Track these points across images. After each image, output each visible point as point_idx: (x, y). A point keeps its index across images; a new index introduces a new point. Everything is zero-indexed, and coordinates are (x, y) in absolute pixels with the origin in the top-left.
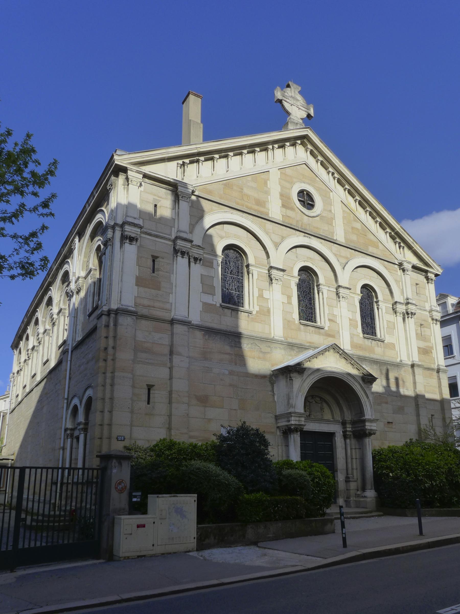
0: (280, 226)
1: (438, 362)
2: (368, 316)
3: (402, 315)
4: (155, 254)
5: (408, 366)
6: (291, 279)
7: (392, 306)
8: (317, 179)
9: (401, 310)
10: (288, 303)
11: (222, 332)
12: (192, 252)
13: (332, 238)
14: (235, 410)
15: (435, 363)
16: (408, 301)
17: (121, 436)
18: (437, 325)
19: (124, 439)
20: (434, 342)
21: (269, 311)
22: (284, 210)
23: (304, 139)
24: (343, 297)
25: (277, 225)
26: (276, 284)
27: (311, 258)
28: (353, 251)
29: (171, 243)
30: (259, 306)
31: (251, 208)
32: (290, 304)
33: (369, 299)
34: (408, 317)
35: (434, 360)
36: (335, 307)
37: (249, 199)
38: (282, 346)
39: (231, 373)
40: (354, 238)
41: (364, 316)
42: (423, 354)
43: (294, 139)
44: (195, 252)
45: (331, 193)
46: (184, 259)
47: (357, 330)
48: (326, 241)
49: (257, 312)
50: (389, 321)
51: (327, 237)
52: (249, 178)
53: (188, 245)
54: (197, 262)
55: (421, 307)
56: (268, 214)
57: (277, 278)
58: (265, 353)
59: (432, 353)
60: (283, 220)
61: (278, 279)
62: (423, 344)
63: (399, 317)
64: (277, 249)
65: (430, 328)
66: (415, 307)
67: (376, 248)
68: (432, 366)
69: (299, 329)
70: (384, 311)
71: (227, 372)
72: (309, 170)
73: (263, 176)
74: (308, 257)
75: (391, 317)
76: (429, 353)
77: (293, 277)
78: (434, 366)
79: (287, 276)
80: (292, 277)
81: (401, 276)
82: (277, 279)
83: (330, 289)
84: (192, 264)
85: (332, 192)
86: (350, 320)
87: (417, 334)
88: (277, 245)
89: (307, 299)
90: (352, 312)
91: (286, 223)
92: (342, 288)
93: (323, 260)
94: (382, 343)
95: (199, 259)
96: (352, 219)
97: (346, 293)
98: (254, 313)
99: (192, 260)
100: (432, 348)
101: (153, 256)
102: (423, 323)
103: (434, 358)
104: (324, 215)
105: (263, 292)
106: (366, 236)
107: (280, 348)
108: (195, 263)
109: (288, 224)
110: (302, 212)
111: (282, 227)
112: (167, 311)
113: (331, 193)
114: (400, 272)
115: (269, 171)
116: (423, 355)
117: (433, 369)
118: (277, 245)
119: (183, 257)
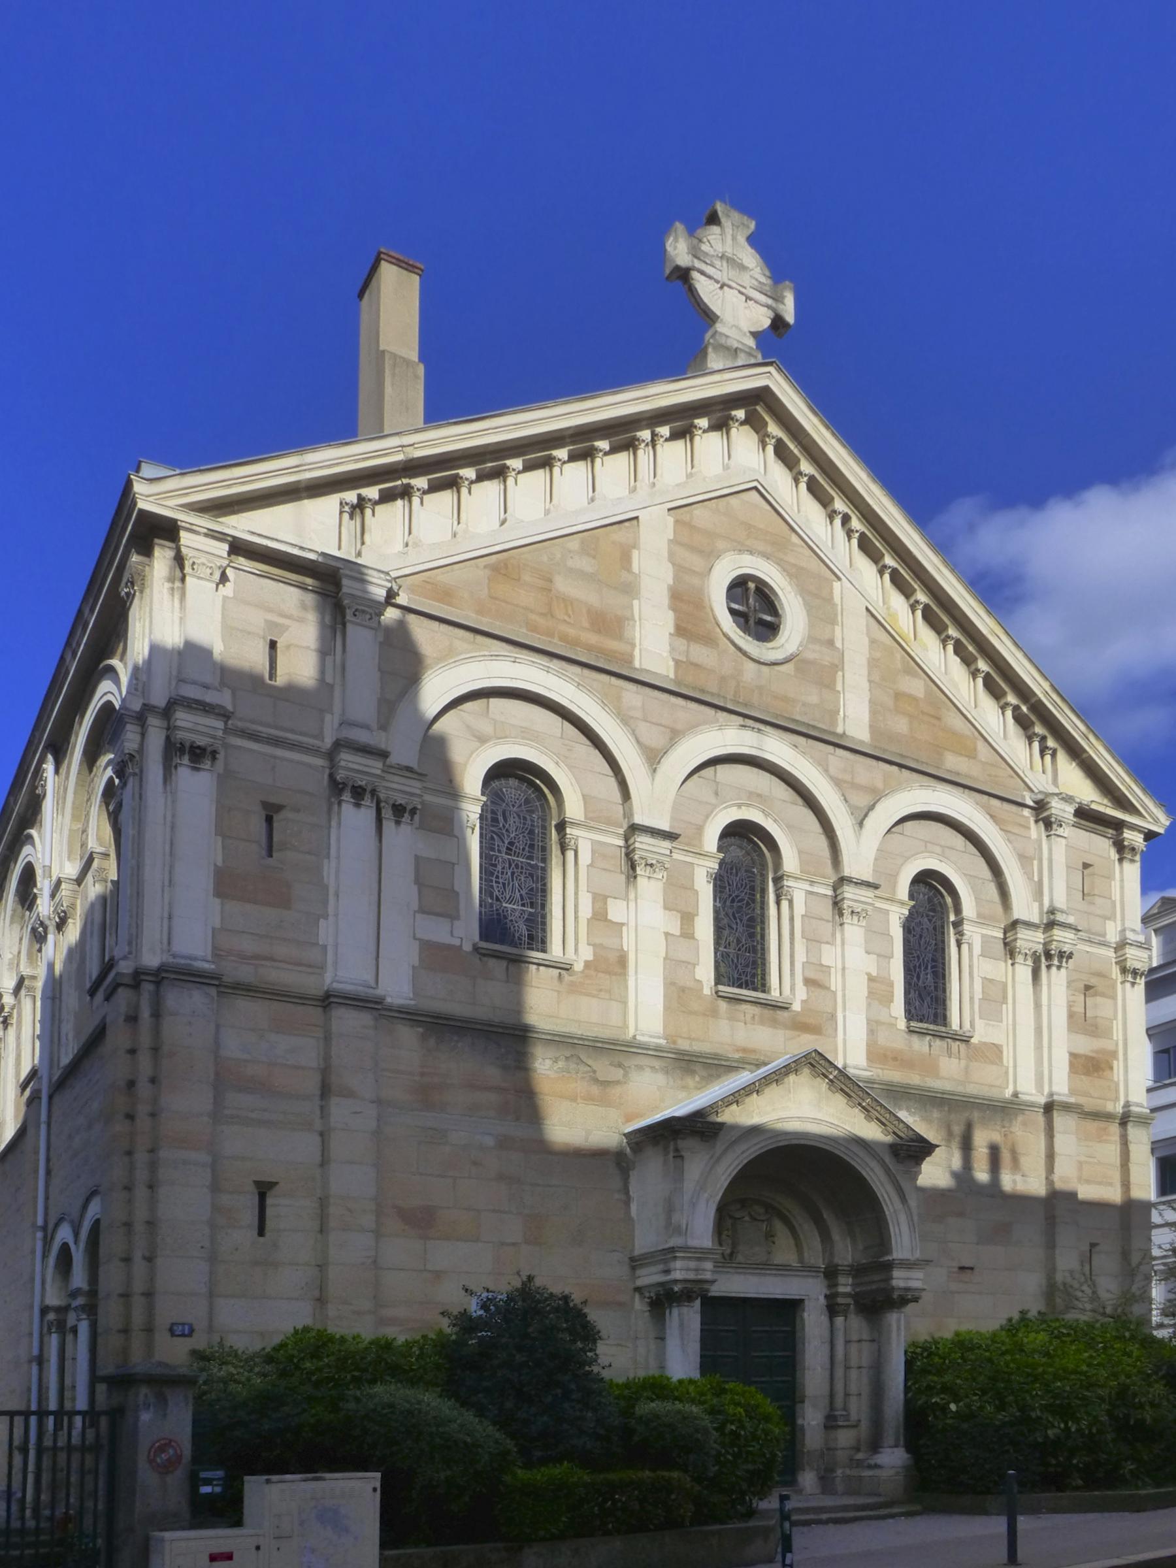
0: (665, 696)
1: (1127, 1095)
2: (926, 968)
3: (1030, 962)
4: (273, 799)
5: (1036, 1109)
6: (695, 861)
7: (1002, 936)
8: (795, 538)
11: (479, 1027)
12: (387, 788)
13: (832, 729)
14: (514, 1244)
15: (1117, 1099)
16: (1052, 917)
17: (183, 1324)
18: (1136, 986)
19: (192, 1331)
20: (1121, 1037)
21: (622, 961)
22: (681, 643)
23: (757, 404)
24: (853, 912)
25: (656, 693)
27: (759, 796)
28: (895, 769)
29: (319, 762)
30: (594, 945)
31: (574, 643)
32: (689, 938)
33: (933, 917)
34: (1049, 967)
35: (1117, 1091)
36: (828, 943)
37: (570, 612)
38: (657, 1064)
39: (504, 1143)
40: (901, 725)
41: (915, 967)
42: (1084, 1074)
43: (722, 407)
44: (397, 788)
45: (837, 585)
46: (363, 809)
47: (889, 1008)
48: (810, 741)
49: (587, 964)
50: (991, 981)
51: (814, 727)
52: (574, 544)
53: (375, 766)
54: (403, 820)
55: (1093, 934)
56: (629, 660)
57: (653, 859)
58: (606, 1084)
59: (1111, 1068)
60: (676, 676)
61: (654, 862)
62: (1086, 1045)
63: (1022, 966)
64: (655, 770)
65: (1114, 997)
66: (1072, 936)
67: (967, 756)
68: (1110, 1107)
69: (714, 1013)
70: (977, 949)
71: (490, 1141)
72: (768, 507)
73: (619, 535)
75: (998, 969)
76: (1103, 1071)
77: (702, 857)
78: (1115, 1107)
79: (685, 853)
80: (698, 856)
81: (1039, 841)
82: (650, 862)
83: (815, 889)
84: (389, 826)
85: (839, 579)
86: (871, 979)
87: (1071, 1015)
88: (654, 758)
89: (741, 920)
90: (879, 955)
91: (687, 686)
92: (852, 885)
93: (799, 801)
94: (963, 1046)
95: (409, 807)
96: (899, 666)
97: (863, 899)
98: (578, 967)
99: (387, 813)
100: (1114, 1054)
101: (266, 805)
103: (1117, 1084)
104: (809, 655)
105: (606, 904)
107: (652, 1068)
108: (398, 823)
109: (694, 688)
110: (739, 649)
111: (673, 699)
112: (309, 970)
113: (837, 585)
114: (1036, 831)
115: (637, 518)
117: (1108, 1117)
118: (654, 758)
119: (358, 805)
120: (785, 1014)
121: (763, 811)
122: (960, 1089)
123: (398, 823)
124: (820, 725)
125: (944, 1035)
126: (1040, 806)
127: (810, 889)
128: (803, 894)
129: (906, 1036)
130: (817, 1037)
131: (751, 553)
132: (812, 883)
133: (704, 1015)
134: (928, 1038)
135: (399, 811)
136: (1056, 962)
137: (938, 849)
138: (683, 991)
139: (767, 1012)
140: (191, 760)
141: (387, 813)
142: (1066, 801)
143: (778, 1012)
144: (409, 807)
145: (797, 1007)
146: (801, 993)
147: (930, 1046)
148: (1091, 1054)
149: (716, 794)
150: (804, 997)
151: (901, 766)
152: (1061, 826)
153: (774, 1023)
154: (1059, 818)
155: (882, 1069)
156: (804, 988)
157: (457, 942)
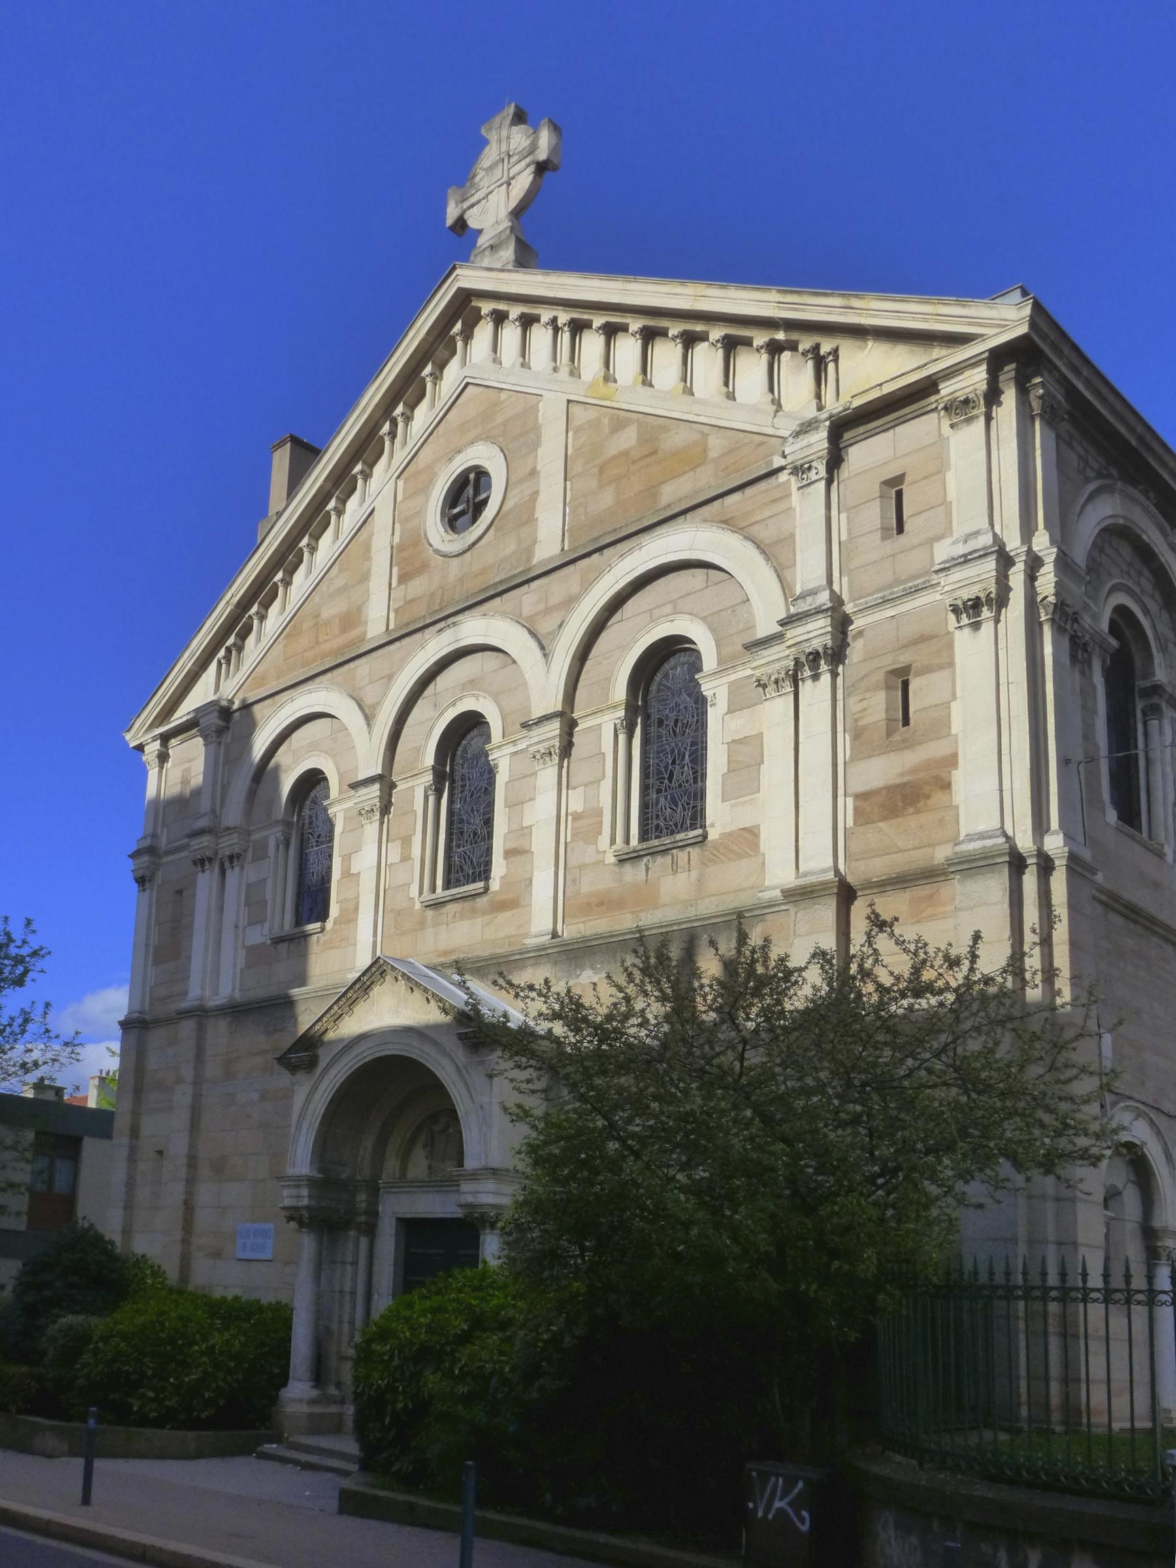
9: (777, 666)
41: (666, 767)
42: (884, 818)
74: (464, 684)
76: (928, 797)
94: (695, 852)
102: (904, 659)
116: (881, 824)
121: (473, 695)
122: (692, 913)
125: (662, 848)
127: (512, 749)
129: (617, 869)
131: (460, 452)
134: (645, 860)
137: (668, 609)
139: (467, 905)
142: (806, 432)
147: (647, 869)
148: (898, 781)
152: (809, 468)
154: (799, 463)
155: (583, 922)
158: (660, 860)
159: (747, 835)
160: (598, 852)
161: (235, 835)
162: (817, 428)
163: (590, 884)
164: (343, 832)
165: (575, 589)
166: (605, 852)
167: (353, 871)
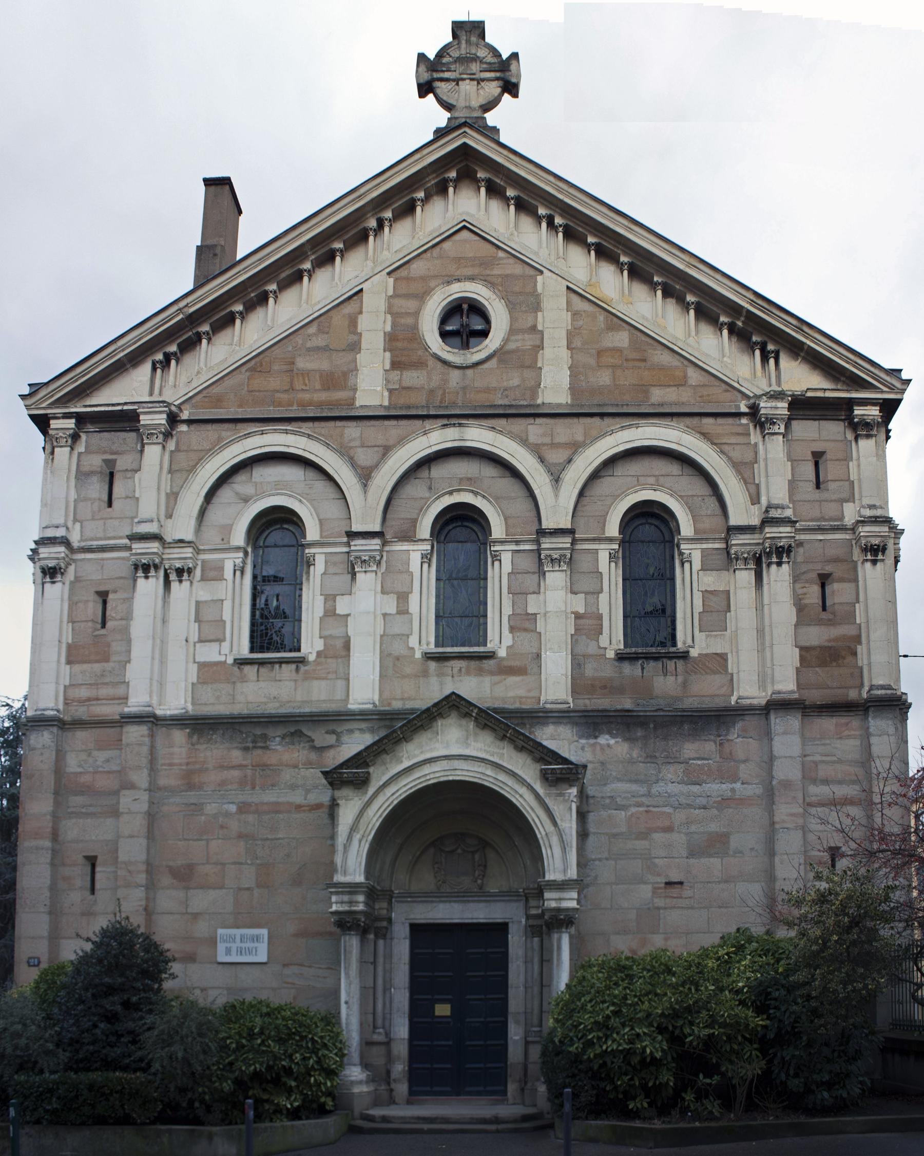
3: (752, 566)
10: (399, 612)
21: (347, 646)
26: (363, 574)
74: (461, 479)
75: (711, 581)
83: (522, 547)
90: (586, 593)
97: (561, 546)
98: (312, 658)
104: (512, 346)
106: (644, 360)
120: (492, 662)
121: (472, 491)
123: (181, 581)
124: (522, 403)
126: (754, 411)
127: (514, 547)
128: (509, 554)
130: (525, 677)
132: (517, 542)
133: (416, 676)
135: (180, 572)
136: (774, 559)
138: (398, 659)
139: (473, 664)
140: (51, 578)
141: (173, 577)
143: (484, 661)
144: (186, 568)
145: (502, 653)
146: (508, 639)
149: (430, 488)
150: (510, 643)
151: (602, 415)
153: (480, 672)
156: (511, 635)
157: (223, 659)
158: (652, 664)
159: (718, 659)
160: (600, 648)
161: (190, 550)
162: (782, 399)
163: (590, 670)
164: (324, 573)
165: (580, 438)
166: (606, 649)
167: (340, 610)
